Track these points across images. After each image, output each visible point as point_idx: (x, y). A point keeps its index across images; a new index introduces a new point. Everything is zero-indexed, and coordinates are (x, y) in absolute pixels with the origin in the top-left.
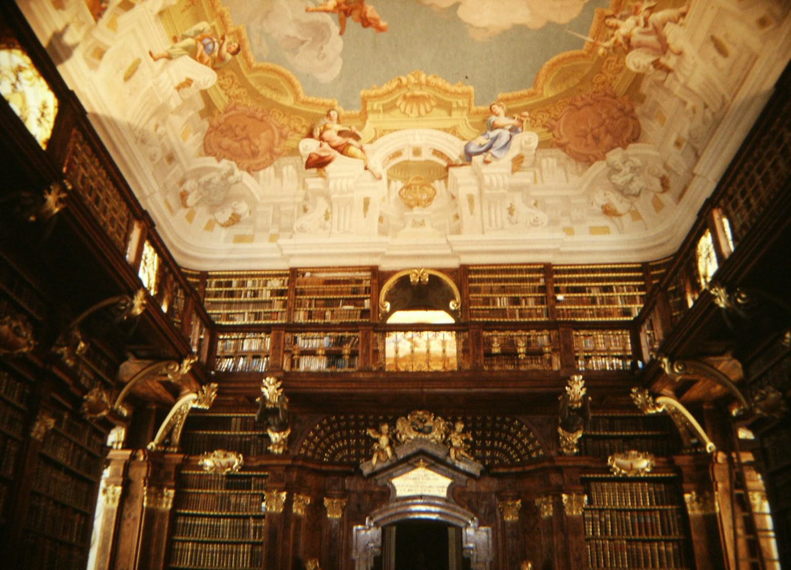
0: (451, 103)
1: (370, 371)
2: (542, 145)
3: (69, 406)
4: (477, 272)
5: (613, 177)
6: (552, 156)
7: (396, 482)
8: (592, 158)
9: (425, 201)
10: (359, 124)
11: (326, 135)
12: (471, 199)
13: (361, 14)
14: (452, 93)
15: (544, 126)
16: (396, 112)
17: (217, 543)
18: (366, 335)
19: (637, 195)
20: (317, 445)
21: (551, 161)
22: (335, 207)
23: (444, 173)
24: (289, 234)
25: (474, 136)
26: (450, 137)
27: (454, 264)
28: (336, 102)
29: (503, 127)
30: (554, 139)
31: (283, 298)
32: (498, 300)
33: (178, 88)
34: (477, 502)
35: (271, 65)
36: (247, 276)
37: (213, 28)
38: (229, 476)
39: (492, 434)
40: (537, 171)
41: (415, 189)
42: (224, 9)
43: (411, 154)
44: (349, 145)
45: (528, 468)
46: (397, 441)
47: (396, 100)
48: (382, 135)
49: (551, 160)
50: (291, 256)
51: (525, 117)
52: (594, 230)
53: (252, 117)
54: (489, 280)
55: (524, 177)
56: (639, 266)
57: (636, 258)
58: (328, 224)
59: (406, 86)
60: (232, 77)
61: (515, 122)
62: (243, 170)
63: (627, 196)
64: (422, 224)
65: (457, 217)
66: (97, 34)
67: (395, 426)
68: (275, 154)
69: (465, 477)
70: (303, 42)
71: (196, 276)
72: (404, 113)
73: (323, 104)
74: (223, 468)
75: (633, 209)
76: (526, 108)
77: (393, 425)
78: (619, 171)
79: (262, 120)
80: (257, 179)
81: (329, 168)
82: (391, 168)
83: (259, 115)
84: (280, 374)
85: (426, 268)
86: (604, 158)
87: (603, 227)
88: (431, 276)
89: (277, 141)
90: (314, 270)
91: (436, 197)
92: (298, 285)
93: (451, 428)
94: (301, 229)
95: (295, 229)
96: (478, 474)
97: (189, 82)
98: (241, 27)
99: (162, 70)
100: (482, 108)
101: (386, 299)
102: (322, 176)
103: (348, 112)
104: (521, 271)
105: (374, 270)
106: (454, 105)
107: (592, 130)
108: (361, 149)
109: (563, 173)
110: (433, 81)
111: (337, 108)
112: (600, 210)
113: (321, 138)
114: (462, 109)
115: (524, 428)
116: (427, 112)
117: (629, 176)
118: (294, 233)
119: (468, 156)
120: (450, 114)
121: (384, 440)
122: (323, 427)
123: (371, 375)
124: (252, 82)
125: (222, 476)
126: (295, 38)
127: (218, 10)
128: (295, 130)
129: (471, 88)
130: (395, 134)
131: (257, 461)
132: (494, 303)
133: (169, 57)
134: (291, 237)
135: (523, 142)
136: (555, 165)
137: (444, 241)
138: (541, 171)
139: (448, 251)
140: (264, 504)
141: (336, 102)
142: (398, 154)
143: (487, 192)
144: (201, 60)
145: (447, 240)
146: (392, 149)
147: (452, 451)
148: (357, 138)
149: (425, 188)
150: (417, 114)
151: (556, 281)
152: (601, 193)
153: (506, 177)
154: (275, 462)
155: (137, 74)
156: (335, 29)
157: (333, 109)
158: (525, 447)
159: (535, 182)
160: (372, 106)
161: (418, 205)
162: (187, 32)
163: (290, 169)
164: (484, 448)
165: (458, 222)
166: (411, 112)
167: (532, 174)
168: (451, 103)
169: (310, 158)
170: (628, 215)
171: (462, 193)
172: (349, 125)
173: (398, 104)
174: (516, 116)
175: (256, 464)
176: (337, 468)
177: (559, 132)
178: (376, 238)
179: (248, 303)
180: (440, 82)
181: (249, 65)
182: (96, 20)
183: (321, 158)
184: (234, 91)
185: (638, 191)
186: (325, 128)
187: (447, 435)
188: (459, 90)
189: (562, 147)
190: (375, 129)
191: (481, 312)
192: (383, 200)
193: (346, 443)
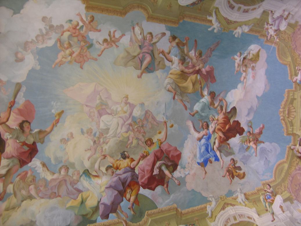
0: (291, 99)
10: (297, 137)
13: (258, 135)
14: (288, 98)
16: (294, 121)
28: (288, 146)
33: (283, 212)
35: (274, 172)
37: (262, 194)
42: (256, 189)
47: (289, 121)
51: (298, 68)
59: (284, 117)
60: (278, 189)
70: (266, 158)
72: (294, 118)
73: (288, 151)
76: (295, 68)
79: (293, 178)
83: (291, 179)
97: (281, 207)
99: (278, 217)
100: (294, 86)
103: (292, 141)
106: (292, 97)
110: (283, 105)
111: (290, 146)
114: (294, 94)
116: (294, 108)
120: (296, 99)
124: (280, 180)
126: (265, 162)
127: (256, 192)
128: (297, 164)
133: (273, 214)
141: (288, 146)
144: (273, 201)
150: (295, 113)
156: (262, 145)
157: (291, 147)
160: (290, 131)
162: (264, 205)
166: (294, 115)
168: (291, 99)
172: (297, 141)
173: (290, 120)
174: (297, 72)
181: (274, 181)
184: (283, 189)
186: (298, 151)
188: (287, 95)
190: (299, 130)
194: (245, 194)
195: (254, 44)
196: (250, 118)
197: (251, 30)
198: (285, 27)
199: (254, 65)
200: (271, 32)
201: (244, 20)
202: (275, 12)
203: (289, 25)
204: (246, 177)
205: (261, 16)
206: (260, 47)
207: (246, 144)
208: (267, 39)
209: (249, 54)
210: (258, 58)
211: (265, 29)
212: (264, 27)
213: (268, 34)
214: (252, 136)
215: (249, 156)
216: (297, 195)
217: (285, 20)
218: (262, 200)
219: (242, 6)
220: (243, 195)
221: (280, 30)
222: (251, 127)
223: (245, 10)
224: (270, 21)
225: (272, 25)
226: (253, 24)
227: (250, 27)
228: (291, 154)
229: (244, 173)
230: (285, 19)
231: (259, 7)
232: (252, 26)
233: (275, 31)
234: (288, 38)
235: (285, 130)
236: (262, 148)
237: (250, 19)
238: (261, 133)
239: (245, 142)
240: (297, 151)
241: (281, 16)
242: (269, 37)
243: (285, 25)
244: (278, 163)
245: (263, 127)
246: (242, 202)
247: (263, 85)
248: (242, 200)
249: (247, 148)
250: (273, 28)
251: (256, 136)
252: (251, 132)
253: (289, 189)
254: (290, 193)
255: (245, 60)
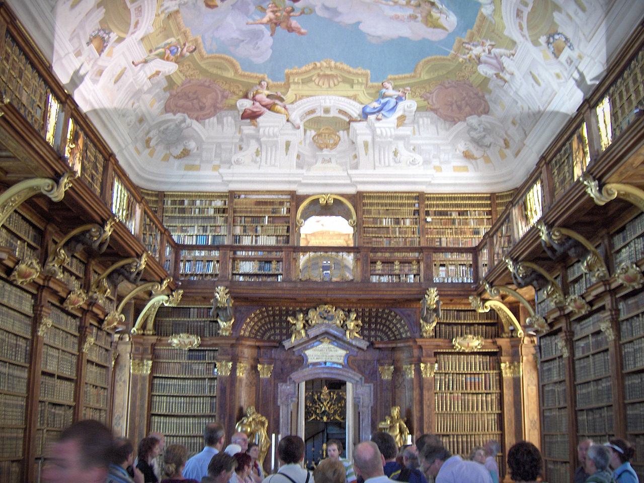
0: (353, 80)
1: (290, 281)
2: (419, 109)
3: (96, 324)
4: (370, 197)
5: (471, 133)
6: (427, 117)
7: (308, 352)
8: (456, 119)
9: (332, 144)
10: (283, 90)
11: (258, 97)
12: (366, 144)
14: (354, 74)
15: (421, 97)
17: (184, 397)
18: (288, 255)
19: (489, 146)
20: (252, 328)
21: (425, 120)
22: (264, 147)
23: (347, 126)
24: (228, 165)
25: (370, 101)
26: (352, 102)
27: (352, 190)
28: (266, 76)
29: (391, 97)
30: (429, 106)
31: (224, 215)
32: (384, 220)
33: (150, 78)
34: (364, 367)
35: (217, 55)
36: (196, 196)
37: (178, 40)
38: (190, 350)
39: (376, 320)
40: (416, 126)
41: (325, 136)
43: (322, 112)
44: (275, 104)
45: (399, 345)
46: (309, 325)
47: (313, 75)
48: (300, 99)
49: (425, 119)
50: (230, 182)
51: (408, 90)
52: (456, 169)
53: (202, 85)
54: (378, 204)
55: (406, 131)
56: (488, 195)
57: (485, 190)
58: (258, 159)
59: (320, 68)
60: (189, 65)
61: (400, 93)
62: (193, 119)
63: (481, 146)
64: (330, 161)
65: (355, 157)
66: (100, 63)
67: (307, 314)
68: (218, 108)
69: (356, 350)
70: (243, 41)
71: (157, 195)
72: (318, 85)
73: (256, 77)
74: (186, 345)
75: (485, 155)
76: (408, 85)
77: (306, 313)
78: (476, 130)
79: (209, 87)
80: (204, 125)
81: (259, 120)
82: (307, 121)
83: (207, 84)
84: (228, 283)
85: (331, 194)
86: (465, 120)
87: (464, 167)
88: (335, 199)
89: (219, 100)
90: (247, 192)
91: (340, 142)
92: (236, 205)
93: (348, 316)
94: (238, 162)
95: (233, 162)
96: (365, 348)
97: (158, 73)
98: (198, 37)
100: (376, 84)
101: (301, 218)
102: (254, 125)
103: (275, 83)
104: (402, 198)
105: (292, 194)
106: (356, 81)
107: (456, 102)
108: (285, 107)
109: (435, 128)
110: (341, 66)
111: (267, 80)
112: (462, 155)
113: (254, 99)
114: (362, 84)
115: (398, 317)
116: (335, 85)
117: (484, 133)
118: (232, 164)
119: (365, 115)
120: (353, 87)
121: (300, 325)
122: (256, 315)
123: (292, 285)
124: (204, 66)
125: (185, 351)
126: (237, 39)
127: (182, 30)
128: (234, 92)
129: (369, 72)
130: (311, 98)
131: (210, 340)
132: (381, 222)
133: (146, 62)
134: (230, 168)
135: (406, 107)
136: (429, 122)
137: (345, 174)
138: (418, 127)
139: (349, 182)
140: (216, 370)
142: (313, 111)
143: (378, 139)
144: (168, 59)
145: (348, 174)
146: (308, 108)
147: (348, 332)
148: (282, 100)
149: (333, 136)
150: (327, 86)
151: (427, 206)
152: (463, 143)
153: (392, 130)
154: (223, 341)
155: (124, 76)
156: (267, 33)
157: (264, 81)
158: (398, 329)
159: (414, 133)
160: (294, 79)
161: (327, 147)
162: (159, 46)
163: (229, 120)
164: (370, 329)
165: (356, 160)
167: (412, 128)
168: (353, 80)
169: (245, 111)
170: (482, 159)
171: (360, 140)
173: (313, 79)
174: (401, 90)
175: (209, 343)
176: (267, 344)
177: (432, 101)
178: (295, 171)
179: (197, 218)
180: (345, 67)
181: (202, 57)
182: (100, 55)
183: (253, 112)
185: (489, 144)
186: (257, 93)
187: (344, 322)
188: (360, 72)
189: (435, 111)
191: (371, 229)
192: (301, 143)
193: (272, 325)
194: (177, 12)
195: (458, 22)
196: (319, 12)
197: (484, 18)
198: (482, 73)
199: (420, 18)
200: (477, 51)
201: (503, 8)
202: (512, 60)
203: (486, 80)
204: (209, 10)
205: (507, 37)
206: (451, 30)
207: (270, 6)
208: (464, 43)
209: (440, 12)
210: (431, 27)
211: (484, 41)
212: (487, 40)
213: (473, 45)
214: (284, 16)
215: (247, 13)
216: (179, 97)
217: (495, 74)
218: (169, 41)
219: (529, 9)
220: (176, 8)
221: (478, 64)
222: (303, 13)
223: (522, 12)
224: (495, 51)
225: (490, 52)
226: (494, 22)
227: (490, 18)
228: (251, 81)
229: (216, 6)
230: (497, 75)
231: (524, 36)
232: (491, 22)
233: (478, 58)
234: (463, 77)
235: (295, 71)
236: (263, 33)
237: (504, 19)
238: (290, 29)
239: (274, 5)
240: (257, 91)
241: (503, 69)
242: (467, 46)
243: (486, 74)
244: (235, 61)
245: (302, 34)
246: (163, 8)
247: (379, 33)
248: (166, 9)
249: (262, 8)
250: (483, 54)
251: (284, 22)
252: (292, 14)
253: (190, 82)
254: (182, 86)
255: (430, 5)
